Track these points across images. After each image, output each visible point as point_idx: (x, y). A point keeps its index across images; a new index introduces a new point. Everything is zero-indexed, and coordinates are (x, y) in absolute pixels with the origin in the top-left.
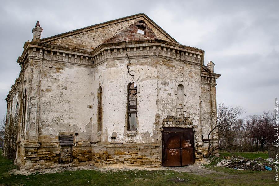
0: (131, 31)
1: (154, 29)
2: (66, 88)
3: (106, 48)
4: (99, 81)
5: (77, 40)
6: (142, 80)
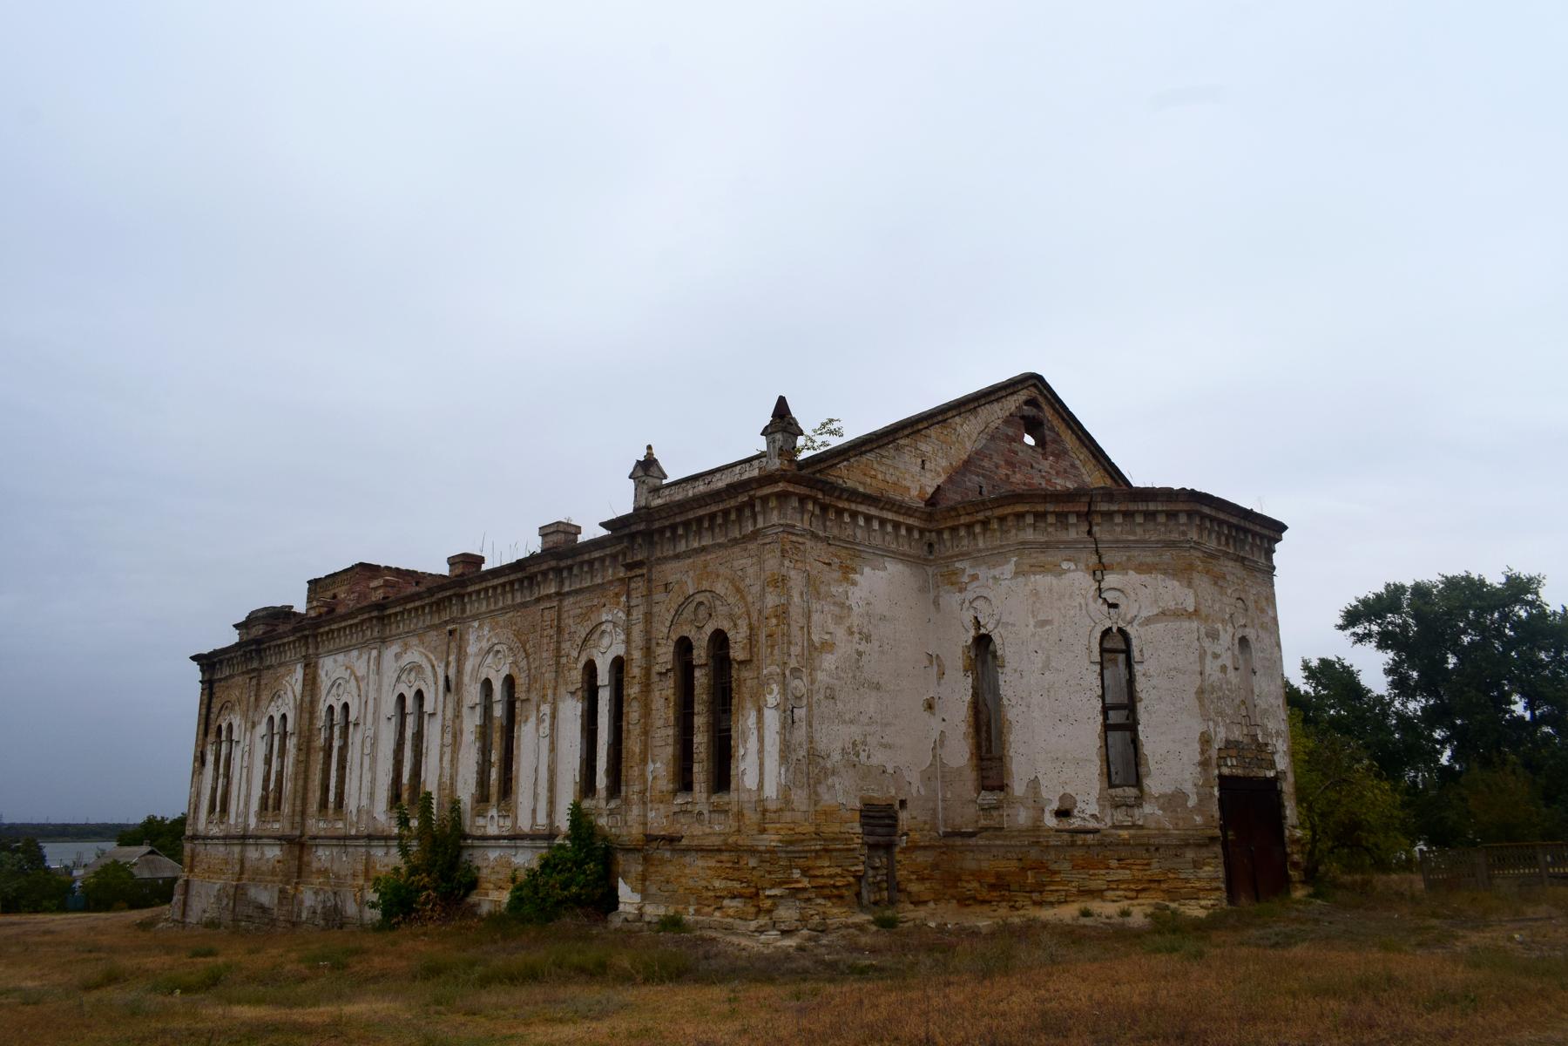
0: (1004, 437)
1: (1061, 428)
2: (868, 639)
3: (1020, 508)
4: (972, 612)
5: (883, 468)
6: (1148, 621)
